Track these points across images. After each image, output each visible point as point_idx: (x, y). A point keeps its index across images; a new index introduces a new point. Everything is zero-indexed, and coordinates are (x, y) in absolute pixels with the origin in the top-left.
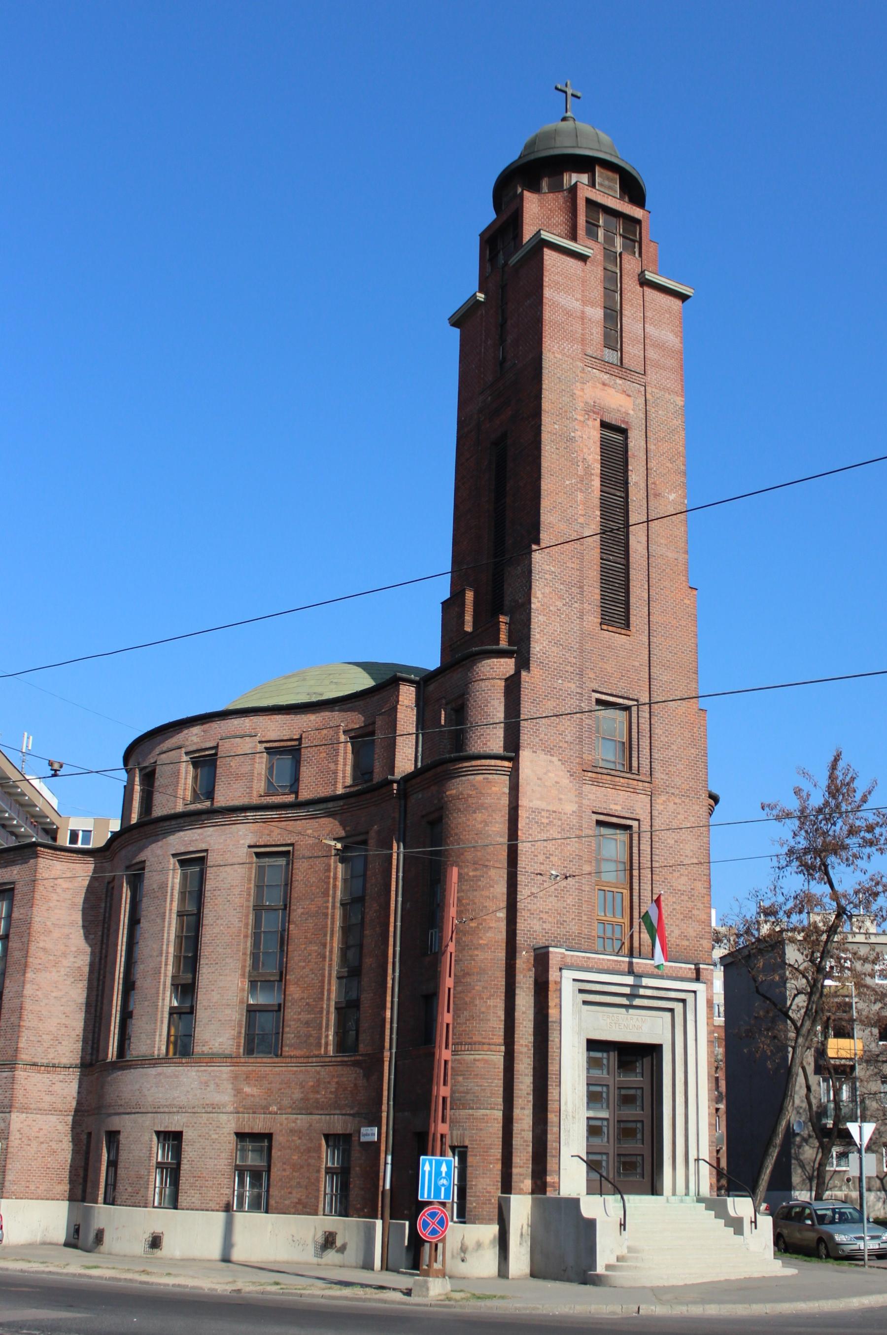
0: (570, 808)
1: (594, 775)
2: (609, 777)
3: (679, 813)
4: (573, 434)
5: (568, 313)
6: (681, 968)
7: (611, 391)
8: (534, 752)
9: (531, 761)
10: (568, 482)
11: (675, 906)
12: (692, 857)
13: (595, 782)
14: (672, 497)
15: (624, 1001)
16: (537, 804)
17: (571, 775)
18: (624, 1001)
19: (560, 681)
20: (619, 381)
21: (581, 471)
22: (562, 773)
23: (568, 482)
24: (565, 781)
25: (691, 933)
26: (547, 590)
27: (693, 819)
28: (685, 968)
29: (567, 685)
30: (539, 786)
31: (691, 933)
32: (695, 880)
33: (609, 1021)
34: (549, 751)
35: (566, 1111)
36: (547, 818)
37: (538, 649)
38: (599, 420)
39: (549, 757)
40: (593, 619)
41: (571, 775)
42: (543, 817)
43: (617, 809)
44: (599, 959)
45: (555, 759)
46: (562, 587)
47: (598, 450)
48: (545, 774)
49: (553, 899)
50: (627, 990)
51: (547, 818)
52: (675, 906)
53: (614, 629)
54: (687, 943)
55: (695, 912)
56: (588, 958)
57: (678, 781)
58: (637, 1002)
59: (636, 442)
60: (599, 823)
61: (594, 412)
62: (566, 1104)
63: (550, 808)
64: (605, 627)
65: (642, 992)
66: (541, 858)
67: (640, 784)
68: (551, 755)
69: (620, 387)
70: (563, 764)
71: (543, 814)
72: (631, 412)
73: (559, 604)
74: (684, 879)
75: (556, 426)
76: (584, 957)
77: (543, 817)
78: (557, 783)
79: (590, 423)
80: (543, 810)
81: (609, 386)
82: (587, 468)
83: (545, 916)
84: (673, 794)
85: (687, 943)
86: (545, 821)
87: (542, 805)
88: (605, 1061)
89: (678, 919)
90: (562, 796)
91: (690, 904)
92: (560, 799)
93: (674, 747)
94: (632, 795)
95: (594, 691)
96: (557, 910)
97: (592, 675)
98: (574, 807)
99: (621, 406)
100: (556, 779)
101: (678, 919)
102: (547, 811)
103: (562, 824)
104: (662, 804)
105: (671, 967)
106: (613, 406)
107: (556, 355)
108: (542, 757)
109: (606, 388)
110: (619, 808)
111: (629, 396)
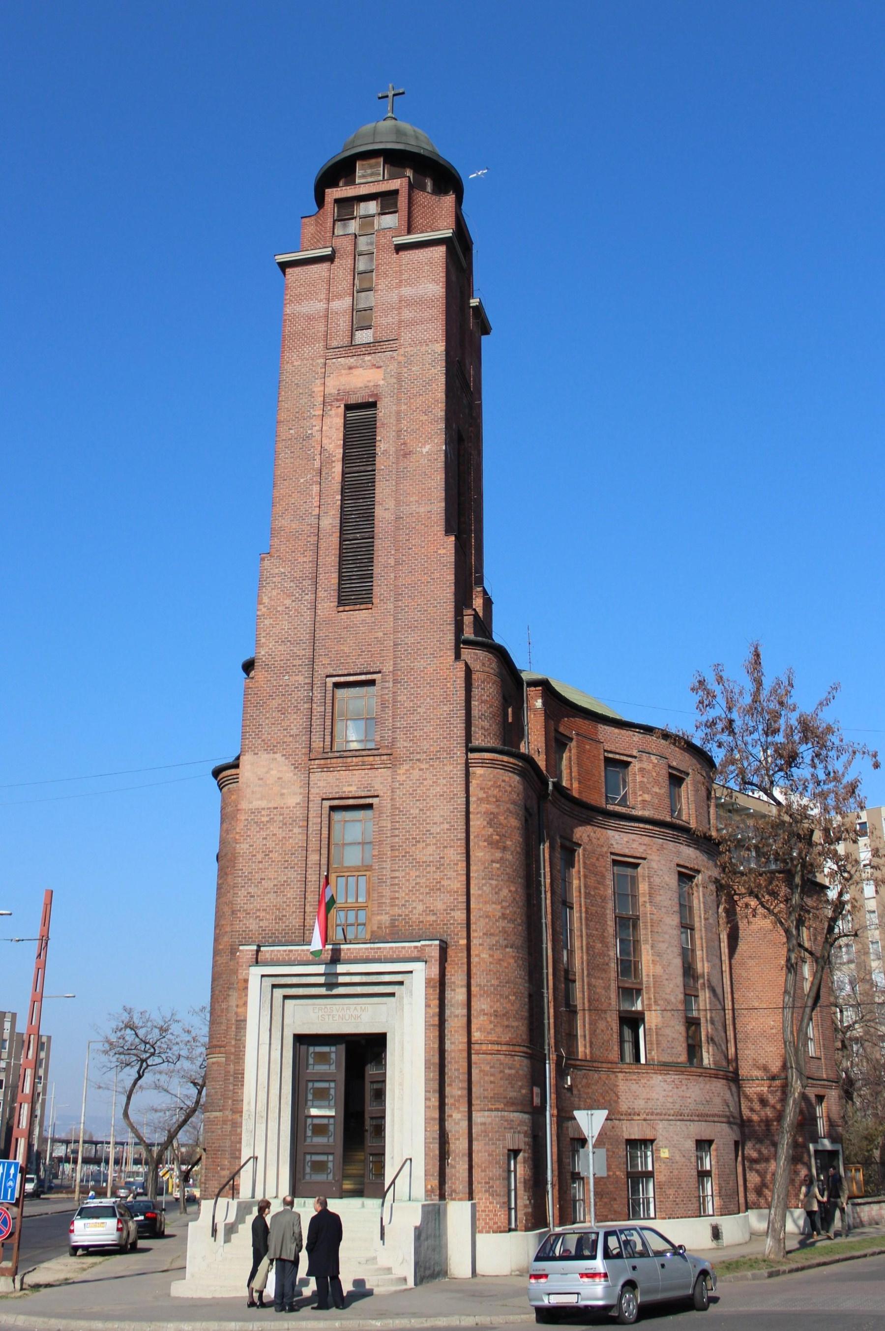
0: (293, 800)
1: (322, 762)
2: (340, 760)
3: (426, 779)
4: (309, 432)
5: (310, 318)
6: (403, 948)
7: (360, 371)
8: (255, 754)
9: (252, 764)
10: (302, 480)
11: (418, 880)
12: (443, 823)
13: (324, 768)
14: (425, 450)
15: (323, 991)
16: (257, 804)
17: (295, 768)
18: (323, 991)
19: (287, 677)
20: (367, 358)
21: (317, 464)
22: (285, 768)
23: (302, 480)
24: (289, 774)
25: (440, 906)
26: (274, 593)
27: (444, 781)
28: (410, 947)
29: (297, 678)
30: (260, 786)
31: (440, 906)
32: (446, 847)
33: (320, 1014)
34: (271, 749)
35: (248, 1110)
36: (268, 815)
37: (263, 653)
38: (342, 406)
39: (272, 755)
40: (328, 604)
41: (295, 768)
42: (263, 816)
43: (352, 790)
44: (303, 950)
45: (278, 756)
46: (292, 584)
47: (341, 435)
48: (267, 772)
49: (272, 896)
50: (322, 980)
51: (268, 815)
52: (418, 880)
53: (352, 607)
54: (434, 918)
55: (445, 883)
56: (291, 951)
57: (425, 745)
58: (336, 991)
59: (384, 412)
60: (333, 808)
61: (337, 400)
62: (249, 1103)
63: (271, 805)
64: (341, 609)
65: (341, 979)
66: (260, 857)
67: (377, 758)
68: (274, 753)
69: (369, 364)
70: (286, 758)
71: (263, 813)
72: (381, 383)
73: (288, 602)
74: (431, 849)
75: (291, 431)
76: (285, 951)
77: (263, 816)
78: (279, 778)
79: (333, 412)
80: (264, 809)
81: (357, 367)
82: (327, 461)
83: (262, 914)
84: (419, 760)
85: (434, 918)
86: (265, 819)
87: (263, 804)
88: (333, 1056)
89: (422, 893)
90: (285, 791)
91: (437, 876)
92: (282, 794)
94: (370, 772)
95: (327, 676)
96: (275, 906)
97: (326, 661)
98: (298, 799)
99: (369, 381)
100: (279, 775)
101: (422, 893)
102: (268, 809)
103: (284, 818)
104: (404, 774)
105: (391, 948)
106: (360, 385)
107: (296, 363)
108: (264, 756)
109: (351, 371)
110: (353, 789)
111: (378, 367)
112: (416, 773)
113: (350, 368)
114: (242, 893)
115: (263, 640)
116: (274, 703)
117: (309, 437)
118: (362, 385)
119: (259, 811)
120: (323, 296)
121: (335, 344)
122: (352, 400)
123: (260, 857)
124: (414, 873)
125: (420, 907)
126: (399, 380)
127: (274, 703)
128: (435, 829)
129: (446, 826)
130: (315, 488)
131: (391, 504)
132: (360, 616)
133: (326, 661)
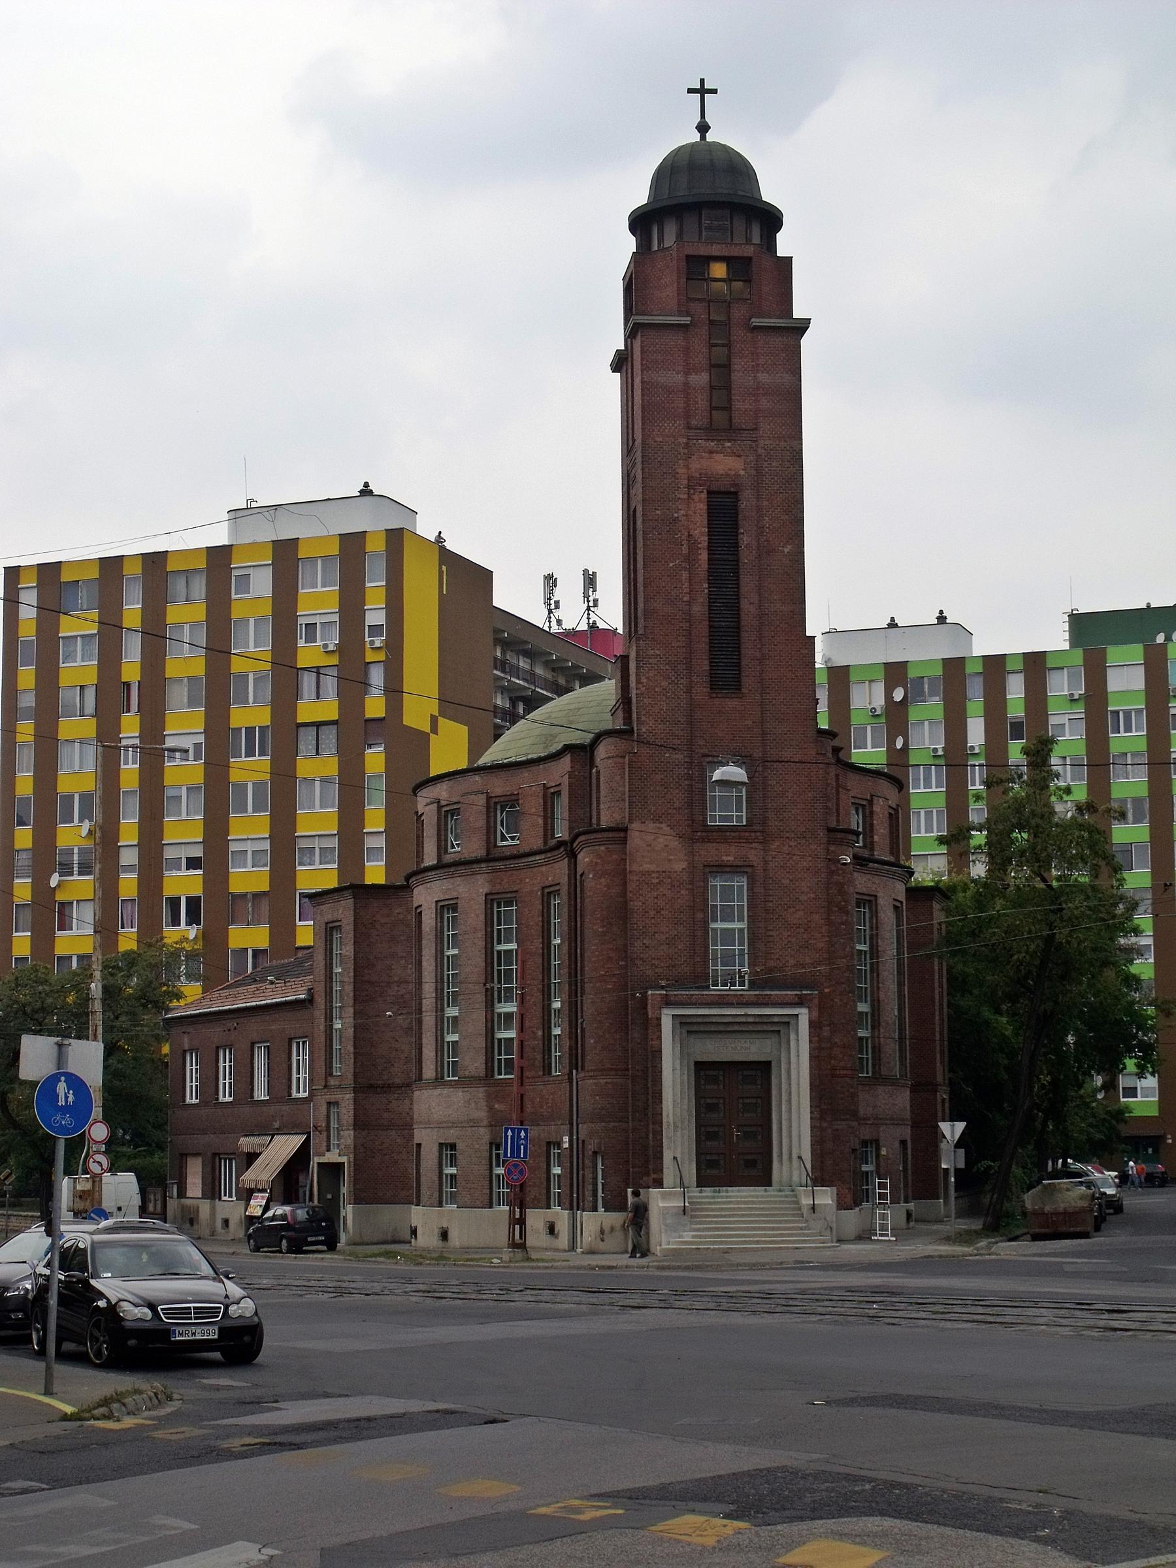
0: (680, 866)
14: (786, 550)
16: (647, 867)
24: (675, 843)
26: (651, 674)
34: (657, 819)
40: (701, 690)
45: (663, 825)
49: (665, 947)
59: (746, 502)
66: (652, 913)
72: (742, 473)
79: (696, 497)
87: (653, 867)
92: (670, 860)
93: (790, 794)
97: (702, 743)
98: (684, 865)
107: (658, 439)
108: (651, 826)
110: (731, 858)
111: (739, 456)
112: (786, 849)
113: (711, 452)
114: (638, 943)
115: (643, 718)
116: (658, 777)
117: (676, 520)
118: (721, 472)
119: (649, 873)
120: (680, 368)
121: (694, 423)
122: (714, 488)
123: (652, 913)
124: (786, 934)
125: (792, 962)
126: (758, 470)
127: (658, 777)
128: (803, 898)
129: (812, 896)
130: (685, 575)
131: (754, 597)
132: (732, 703)
133: (702, 743)
